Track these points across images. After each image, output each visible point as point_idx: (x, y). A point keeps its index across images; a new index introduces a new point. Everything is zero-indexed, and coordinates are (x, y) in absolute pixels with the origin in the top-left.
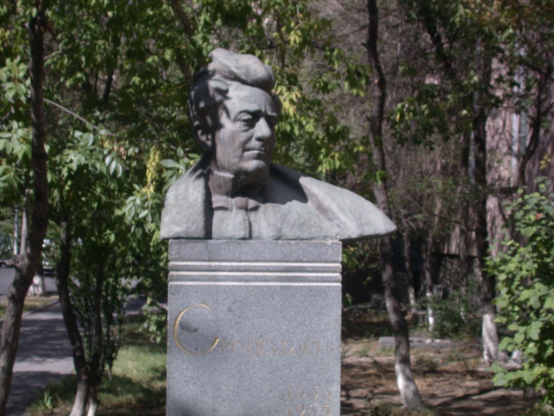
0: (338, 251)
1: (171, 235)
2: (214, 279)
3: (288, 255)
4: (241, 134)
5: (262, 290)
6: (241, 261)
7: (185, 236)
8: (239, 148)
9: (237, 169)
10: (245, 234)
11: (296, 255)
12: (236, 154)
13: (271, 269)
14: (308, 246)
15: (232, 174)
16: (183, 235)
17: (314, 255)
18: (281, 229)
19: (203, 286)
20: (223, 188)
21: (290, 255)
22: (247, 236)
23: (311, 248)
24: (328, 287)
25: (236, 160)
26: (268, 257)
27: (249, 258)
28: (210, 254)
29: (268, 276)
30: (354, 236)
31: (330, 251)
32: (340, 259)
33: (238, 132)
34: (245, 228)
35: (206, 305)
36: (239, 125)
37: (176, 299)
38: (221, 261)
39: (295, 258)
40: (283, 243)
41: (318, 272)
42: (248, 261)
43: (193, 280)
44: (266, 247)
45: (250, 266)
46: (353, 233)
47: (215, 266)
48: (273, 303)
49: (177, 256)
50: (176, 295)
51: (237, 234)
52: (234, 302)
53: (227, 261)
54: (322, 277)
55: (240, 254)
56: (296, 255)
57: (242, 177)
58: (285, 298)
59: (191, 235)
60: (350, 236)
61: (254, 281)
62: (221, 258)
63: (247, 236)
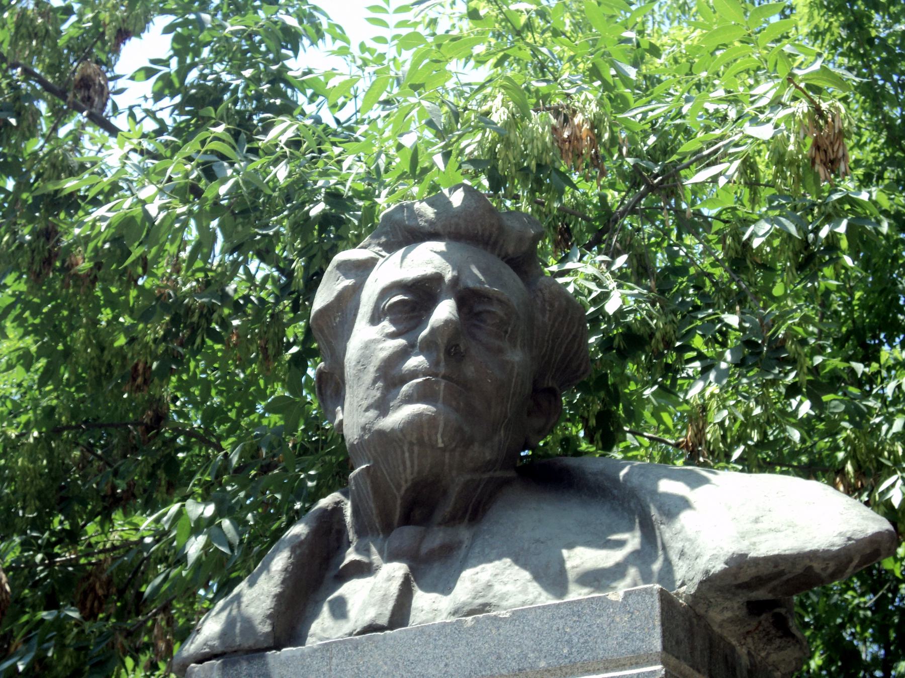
0: (649, 617)
4: (380, 346)
8: (375, 381)
10: (379, 615)
11: (516, 651)
12: (370, 401)
14: (553, 618)
17: (569, 642)
18: (489, 586)
21: (499, 658)
22: (384, 621)
23: (561, 623)
30: (718, 566)
31: (623, 620)
32: (657, 644)
33: (375, 341)
34: (384, 598)
36: (387, 326)
40: (477, 621)
44: (427, 643)
46: (714, 557)
60: (707, 572)
63: (384, 621)
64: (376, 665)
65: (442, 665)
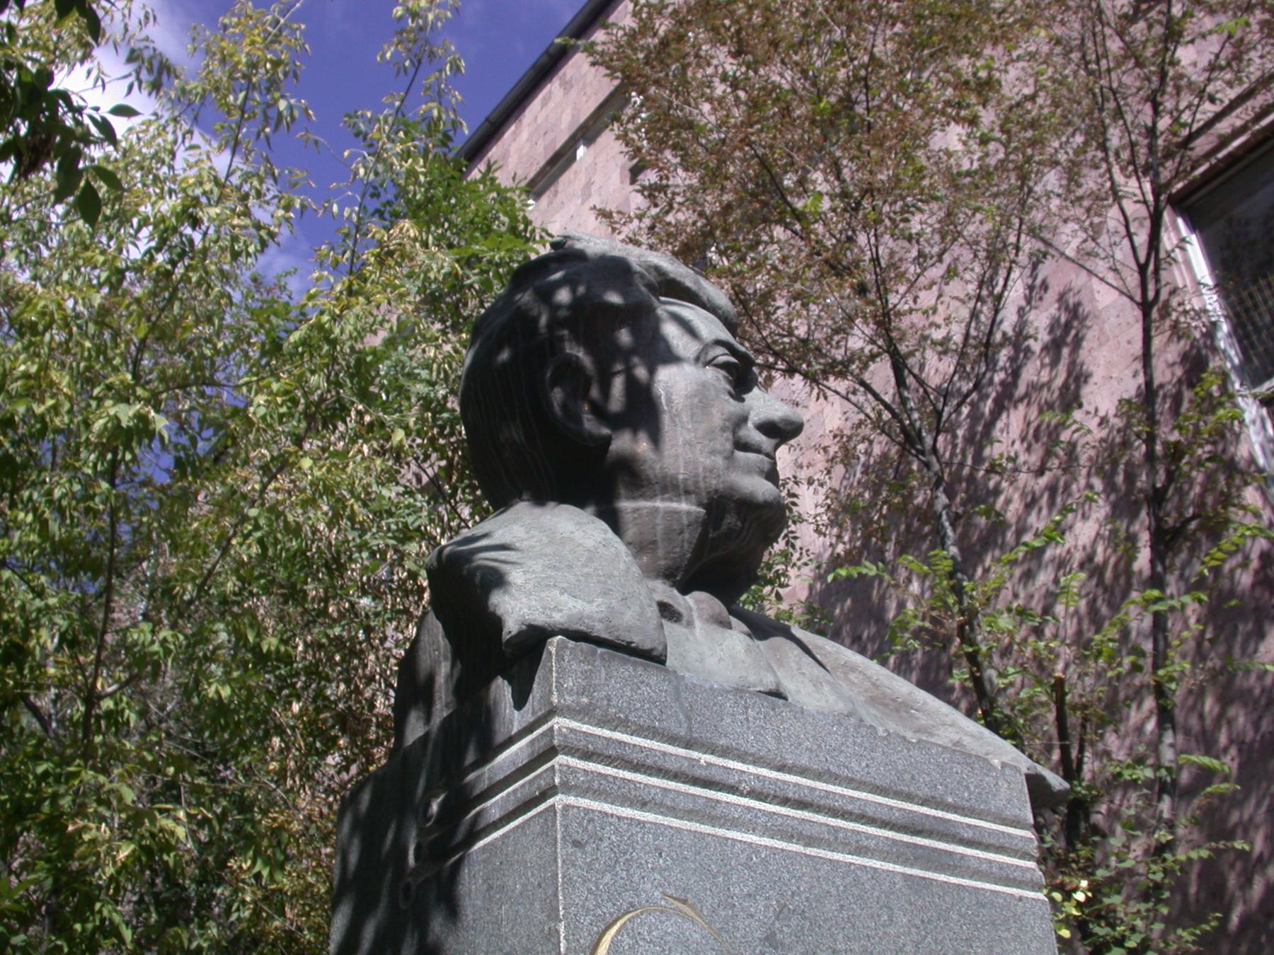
1: (558, 618)
2: (707, 814)
3: (907, 777)
5: (857, 881)
6: (781, 768)
7: (604, 635)
8: (723, 429)
9: (721, 486)
13: (870, 812)
15: (700, 504)
16: (600, 630)
19: (679, 830)
20: (661, 552)
21: (913, 778)
24: (1021, 899)
25: (719, 461)
26: (857, 769)
27: (804, 761)
28: (689, 718)
29: (868, 836)
35: (692, 907)
37: (590, 867)
38: (725, 752)
39: (925, 792)
41: (987, 848)
42: (803, 772)
43: (643, 805)
45: (812, 789)
47: (709, 764)
48: (891, 930)
49: (585, 700)
50: (588, 848)
51: (752, 678)
52: (782, 912)
53: (742, 757)
54: (1001, 866)
55: (778, 740)
56: (928, 779)
57: (730, 520)
58: (923, 922)
59: (626, 637)
61: (830, 846)
62: (722, 742)
64: (798, 736)
65: (864, 764)
